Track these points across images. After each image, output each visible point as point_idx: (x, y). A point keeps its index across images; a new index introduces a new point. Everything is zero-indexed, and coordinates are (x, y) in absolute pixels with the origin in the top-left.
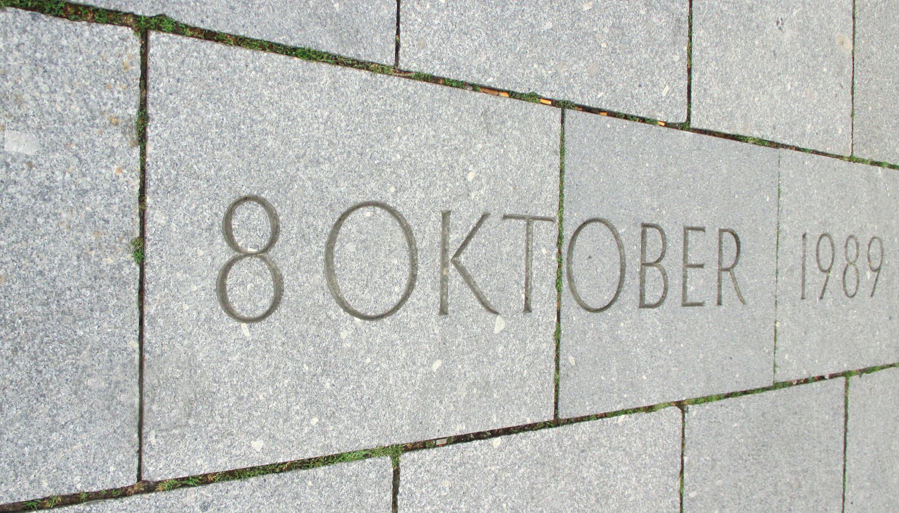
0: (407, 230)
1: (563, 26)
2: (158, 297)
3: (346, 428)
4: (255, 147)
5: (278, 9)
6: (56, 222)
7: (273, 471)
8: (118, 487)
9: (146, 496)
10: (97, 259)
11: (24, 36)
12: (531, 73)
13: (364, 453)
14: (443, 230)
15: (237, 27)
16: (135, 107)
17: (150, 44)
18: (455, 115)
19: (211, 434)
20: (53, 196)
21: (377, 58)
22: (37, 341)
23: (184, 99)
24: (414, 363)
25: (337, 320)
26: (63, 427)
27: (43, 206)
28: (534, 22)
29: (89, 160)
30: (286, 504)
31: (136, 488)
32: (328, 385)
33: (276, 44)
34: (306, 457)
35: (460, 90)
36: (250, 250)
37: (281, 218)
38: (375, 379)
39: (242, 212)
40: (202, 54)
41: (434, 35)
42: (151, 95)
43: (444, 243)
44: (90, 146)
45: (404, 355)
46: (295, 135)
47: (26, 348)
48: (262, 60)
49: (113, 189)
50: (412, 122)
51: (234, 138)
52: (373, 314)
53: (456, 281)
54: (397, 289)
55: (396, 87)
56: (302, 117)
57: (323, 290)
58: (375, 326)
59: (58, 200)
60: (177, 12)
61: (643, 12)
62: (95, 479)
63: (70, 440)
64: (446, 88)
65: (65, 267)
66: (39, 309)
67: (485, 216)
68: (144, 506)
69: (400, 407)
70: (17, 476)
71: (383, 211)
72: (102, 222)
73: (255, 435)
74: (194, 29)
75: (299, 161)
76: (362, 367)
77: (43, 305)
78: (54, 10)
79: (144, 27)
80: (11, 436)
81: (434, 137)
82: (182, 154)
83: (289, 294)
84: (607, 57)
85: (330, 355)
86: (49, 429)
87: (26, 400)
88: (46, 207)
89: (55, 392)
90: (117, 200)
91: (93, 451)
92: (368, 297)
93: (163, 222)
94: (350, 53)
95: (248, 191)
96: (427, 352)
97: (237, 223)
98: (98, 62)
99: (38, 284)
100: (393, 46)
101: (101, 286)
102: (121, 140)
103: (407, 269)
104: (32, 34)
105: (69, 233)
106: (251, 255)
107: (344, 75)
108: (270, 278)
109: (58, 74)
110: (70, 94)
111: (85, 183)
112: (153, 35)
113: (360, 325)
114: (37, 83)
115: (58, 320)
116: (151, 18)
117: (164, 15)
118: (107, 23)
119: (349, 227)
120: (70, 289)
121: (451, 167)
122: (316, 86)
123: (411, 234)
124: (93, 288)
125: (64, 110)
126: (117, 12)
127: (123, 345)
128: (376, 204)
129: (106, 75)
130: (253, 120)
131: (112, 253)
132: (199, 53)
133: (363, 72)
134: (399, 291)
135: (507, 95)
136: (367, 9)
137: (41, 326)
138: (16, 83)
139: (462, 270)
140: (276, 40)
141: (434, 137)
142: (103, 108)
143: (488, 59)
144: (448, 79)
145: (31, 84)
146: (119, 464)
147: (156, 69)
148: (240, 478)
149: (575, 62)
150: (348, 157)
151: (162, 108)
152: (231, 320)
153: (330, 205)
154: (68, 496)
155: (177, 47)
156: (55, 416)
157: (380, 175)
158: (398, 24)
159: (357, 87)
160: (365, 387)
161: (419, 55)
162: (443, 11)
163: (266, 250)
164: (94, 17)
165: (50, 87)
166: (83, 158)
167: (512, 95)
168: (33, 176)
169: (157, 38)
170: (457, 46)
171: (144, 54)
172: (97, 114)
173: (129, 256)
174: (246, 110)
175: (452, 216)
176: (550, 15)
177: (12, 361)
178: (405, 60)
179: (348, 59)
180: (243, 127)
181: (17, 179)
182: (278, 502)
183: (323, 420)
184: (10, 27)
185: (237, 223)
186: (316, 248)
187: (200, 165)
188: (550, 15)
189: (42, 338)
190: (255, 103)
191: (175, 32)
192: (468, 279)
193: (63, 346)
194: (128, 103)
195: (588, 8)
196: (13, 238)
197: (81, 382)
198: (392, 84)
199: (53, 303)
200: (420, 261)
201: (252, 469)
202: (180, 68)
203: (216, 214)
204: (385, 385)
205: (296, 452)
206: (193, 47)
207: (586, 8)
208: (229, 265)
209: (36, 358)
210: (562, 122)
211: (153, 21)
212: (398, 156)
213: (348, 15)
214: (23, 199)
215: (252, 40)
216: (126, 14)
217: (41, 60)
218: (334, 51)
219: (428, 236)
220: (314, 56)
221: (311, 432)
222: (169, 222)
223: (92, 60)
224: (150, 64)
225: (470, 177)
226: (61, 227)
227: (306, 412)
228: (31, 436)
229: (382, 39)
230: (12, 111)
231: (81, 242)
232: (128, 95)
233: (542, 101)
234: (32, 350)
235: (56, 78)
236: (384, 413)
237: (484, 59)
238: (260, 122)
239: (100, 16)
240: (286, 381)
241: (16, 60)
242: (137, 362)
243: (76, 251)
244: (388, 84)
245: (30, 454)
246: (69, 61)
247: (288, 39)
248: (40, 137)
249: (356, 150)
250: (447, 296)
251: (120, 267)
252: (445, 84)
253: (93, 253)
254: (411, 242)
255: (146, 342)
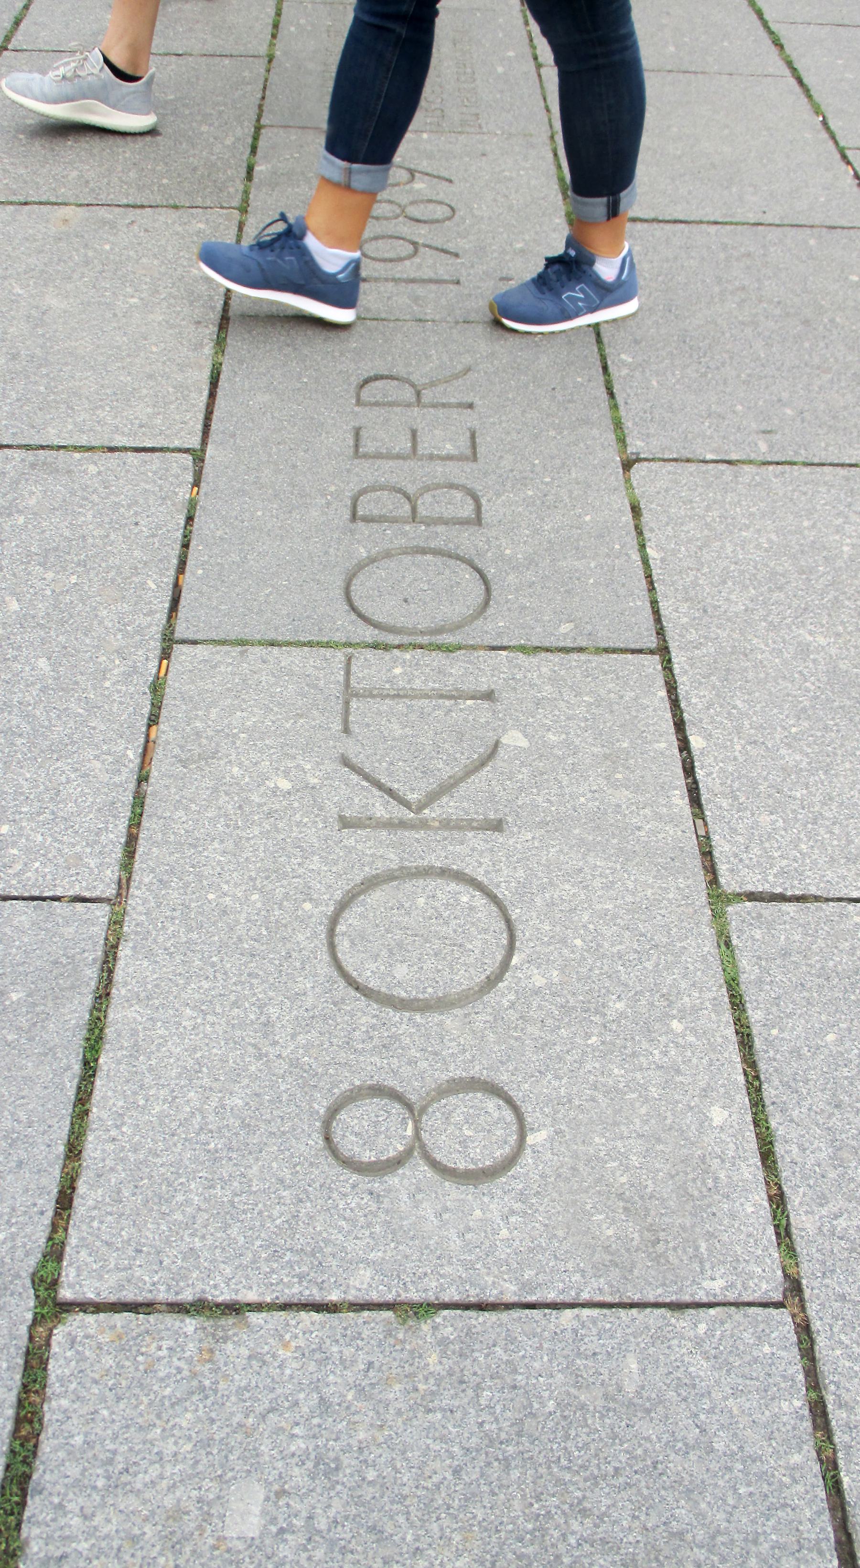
0: (370, 884)
1: (43, 642)
2: (490, 1280)
3: (685, 976)
4: (244, 1125)
5: (21, 1090)
6: (373, 1448)
7: (759, 1090)
8: (795, 1339)
9: (807, 1293)
10: (432, 1381)
11: (70, 1506)
12: (119, 692)
13: (723, 948)
14: (369, 826)
15: (52, 1157)
16: (182, 1321)
17: (80, 1298)
18: (187, 809)
19: (704, 1189)
20: (332, 1454)
21: (99, 931)
22: (568, 1477)
23: (168, 1242)
24: (580, 870)
25: (516, 992)
26: (703, 1431)
27: (348, 1471)
28: (38, 686)
29: (272, 1396)
30: (809, 1069)
31: (796, 1311)
32: (620, 1006)
33: (78, 1093)
34: (734, 1038)
35: (148, 801)
36: (409, 1132)
37: (358, 1083)
38: (608, 932)
39: (349, 1145)
40: (95, 1213)
41: (60, 842)
42: (163, 1295)
43: (390, 825)
44: (247, 1395)
45: (567, 887)
46: (224, 1061)
47: (579, 1494)
48: (104, 1115)
49: (318, 1356)
50: (200, 877)
51: (230, 1159)
52: (505, 935)
53: (449, 807)
54: (465, 899)
55: (145, 901)
56: (195, 1050)
57: (469, 1014)
58: (523, 933)
59: (337, 1446)
60: (27, 1254)
61: (21, 520)
62: (783, 1377)
63: (725, 1419)
64: (145, 823)
65: (445, 1432)
66: (515, 1474)
67: (346, 762)
68: (822, 1296)
69: (649, 892)
70: (785, 1505)
71: (341, 921)
72: (371, 1373)
73: (704, 1120)
74: (54, 1227)
75: (266, 1055)
76: (588, 951)
77: (507, 1468)
78: (26, 1457)
79: (52, 1307)
80: (721, 1516)
81: (222, 841)
82: (258, 1243)
83: (477, 1068)
84: (92, 574)
85: (572, 1002)
86: (708, 1453)
87: (663, 1492)
88: (350, 1466)
89: (648, 1445)
90: (335, 1349)
91: (740, 1381)
92: (479, 943)
93: (369, 1273)
94: (91, 974)
95: (315, 1135)
96: (561, 851)
97: (368, 1154)
98: (110, 1383)
99: (474, 1477)
100: (79, 906)
101: (475, 1374)
102: (237, 1344)
103: (432, 883)
104: (66, 1495)
105: (391, 1427)
106: (417, 1130)
107: (126, 984)
108: (453, 1100)
109: (131, 1449)
110: (164, 1430)
111: (308, 1402)
112: (66, 1294)
113: (523, 955)
114: (146, 1485)
115: (532, 1443)
116: (37, 1297)
117: (34, 1274)
118: (45, 1369)
119: (369, 974)
120: (481, 1424)
121: (269, 815)
122: (145, 1029)
123: (376, 876)
124: (478, 1384)
125: (189, 1438)
126: (28, 1353)
127: (569, 1335)
128: (331, 932)
129: (132, 1369)
130: (201, 1129)
131: (420, 1357)
132: (93, 1219)
133: (120, 954)
134: (467, 896)
135: (154, 728)
136: (19, 948)
137: (542, 1470)
138: (146, 1519)
139: (432, 798)
140: (71, 1093)
141: (222, 841)
142: (186, 1373)
143: (97, 757)
144: (130, 819)
145: (148, 1495)
146: (759, 1338)
147: (121, 1287)
148: (771, 1143)
149: (101, 623)
150: (257, 976)
151: (185, 1278)
152: (522, 1161)
153: (335, 1004)
154: (814, 1421)
155: (84, 1253)
156: (686, 1445)
157: (285, 926)
158: (44, 899)
159: (146, 963)
160: (619, 947)
161: (92, 865)
162: (21, 828)
163: (409, 1106)
164: (37, 1392)
165: (152, 1463)
166: (267, 1405)
167: (153, 720)
168: (298, 1488)
169: (71, 1286)
170: (77, 806)
171: (98, 1307)
172: (195, 1383)
173: (425, 1327)
174: (186, 1140)
175: (347, 813)
176: (27, 662)
177: (601, 1517)
178: (101, 886)
179: (101, 978)
180: (212, 1145)
181: (304, 1514)
182: (806, 1081)
183: (675, 1012)
184: (54, 1531)
185: (368, 1154)
186: (404, 1026)
187: (275, 1213)
188: (27, 662)
189: (562, 1468)
190: (174, 1125)
191: (60, 1258)
192: (446, 788)
193: (573, 1433)
194: (176, 1332)
195: (15, 603)
196: (401, 1519)
197: (631, 1404)
198: (140, 908)
199: (504, 1452)
200: (420, 863)
201: (756, 1124)
202: (118, 1249)
203: (354, 1186)
204: (615, 917)
205: (726, 1055)
206: (84, 1227)
207: (14, 606)
208: (435, 1165)
209: (595, 1478)
210: (195, 642)
211: (43, 1293)
212: (255, 897)
213: (29, 978)
214: (337, 1505)
215: (72, 1132)
216: (31, 1338)
217: (109, 1478)
218: (88, 1000)
219: (378, 851)
220: (97, 1031)
221: (694, 1031)
222: (368, 1263)
223: (108, 1393)
224: (113, 1298)
225: (285, 785)
226: (381, 1440)
227: (663, 1039)
228: (721, 1483)
229: (67, 923)
230: (193, 1525)
231: (403, 1407)
232: (164, 1334)
233: (162, 674)
234: (581, 1485)
235: (137, 1454)
236: (659, 918)
237: (98, 765)
238: (203, 1118)
239: (35, 1381)
240: (616, 1071)
241: (108, 1521)
242: (595, 1312)
243: (420, 1415)
244: (141, 914)
245: (749, 1485)
246: (109, 1432)
247: (69, 1073)
248: (235, 1478)
249: (245, 964)
250: (473, 820)
251: (444, 1343)
252: (139, 825)
253: (422, 1387)
254: (390, 877)
255: (560, 1298)
